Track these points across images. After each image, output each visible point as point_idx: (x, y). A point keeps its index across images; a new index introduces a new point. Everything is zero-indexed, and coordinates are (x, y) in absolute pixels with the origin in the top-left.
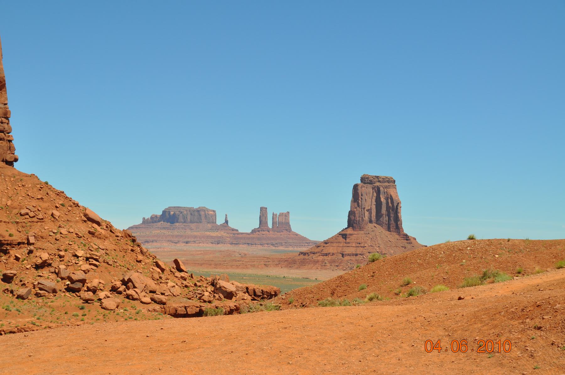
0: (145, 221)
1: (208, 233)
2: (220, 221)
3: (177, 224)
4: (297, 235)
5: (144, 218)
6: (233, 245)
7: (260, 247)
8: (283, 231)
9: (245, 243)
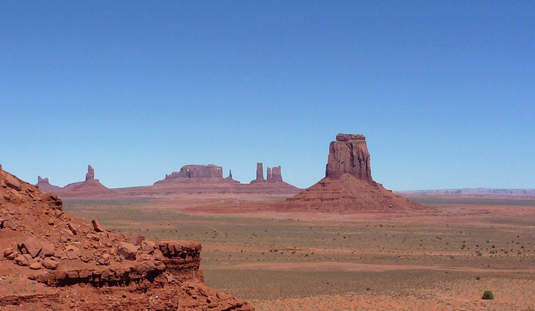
0: (167, 177)
1: (216, 185)
2: (225, 175)
3: (192, 179)
4: (287, 184)
5: (166, 175)
6: (236, 194)
7: (257, 195)
8: (277, 181)
9: (245, 192)
